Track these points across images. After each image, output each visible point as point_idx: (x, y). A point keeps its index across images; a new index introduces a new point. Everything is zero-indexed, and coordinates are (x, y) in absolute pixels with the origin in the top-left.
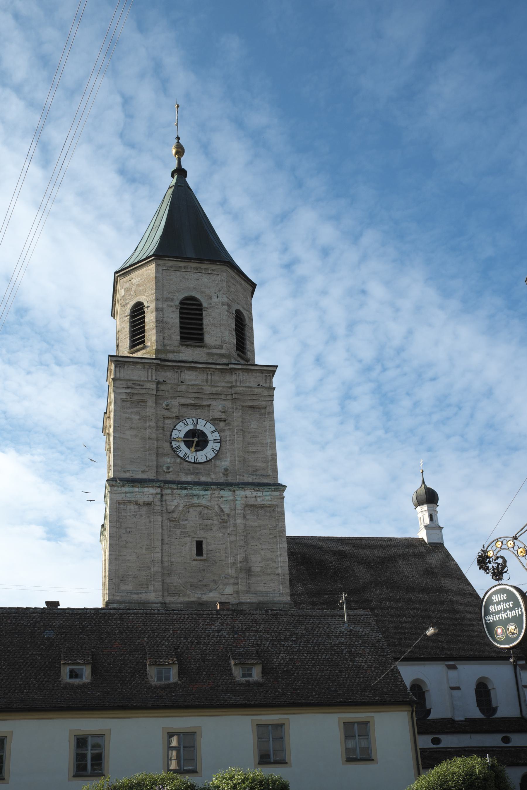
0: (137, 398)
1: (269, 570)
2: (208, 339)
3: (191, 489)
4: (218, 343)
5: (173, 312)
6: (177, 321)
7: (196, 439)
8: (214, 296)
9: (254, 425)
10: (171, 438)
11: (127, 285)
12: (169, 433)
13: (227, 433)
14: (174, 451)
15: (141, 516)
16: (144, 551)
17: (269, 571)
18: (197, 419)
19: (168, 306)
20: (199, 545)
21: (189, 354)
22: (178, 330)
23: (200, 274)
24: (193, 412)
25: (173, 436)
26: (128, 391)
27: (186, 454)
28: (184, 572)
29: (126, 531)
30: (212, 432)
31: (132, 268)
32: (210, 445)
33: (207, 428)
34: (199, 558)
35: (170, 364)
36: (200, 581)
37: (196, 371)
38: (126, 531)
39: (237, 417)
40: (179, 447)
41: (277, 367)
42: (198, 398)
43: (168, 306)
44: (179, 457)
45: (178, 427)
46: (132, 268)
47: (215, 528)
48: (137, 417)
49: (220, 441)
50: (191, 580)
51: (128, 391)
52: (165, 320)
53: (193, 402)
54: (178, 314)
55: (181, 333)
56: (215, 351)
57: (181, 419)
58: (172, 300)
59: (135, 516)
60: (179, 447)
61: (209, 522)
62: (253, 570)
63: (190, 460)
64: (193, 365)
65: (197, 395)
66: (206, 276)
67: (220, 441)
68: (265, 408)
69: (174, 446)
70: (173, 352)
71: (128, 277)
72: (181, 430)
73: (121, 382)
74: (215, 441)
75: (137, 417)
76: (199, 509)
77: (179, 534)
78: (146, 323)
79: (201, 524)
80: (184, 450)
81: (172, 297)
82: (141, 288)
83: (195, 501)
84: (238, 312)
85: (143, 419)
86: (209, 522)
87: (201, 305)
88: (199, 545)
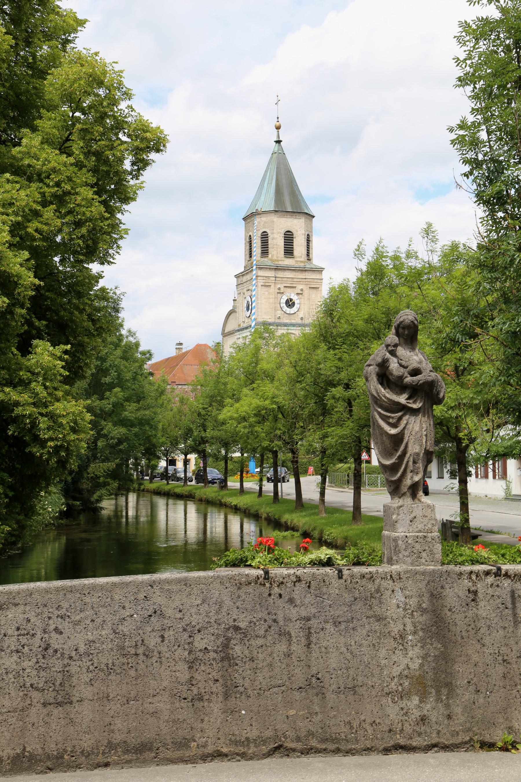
0: (267, 284)
2: (296, 253)
9: (313, 296)
21: (288, 262)
24: (289, 290)
32: (296, 306)
33: (295, 298)
39: (306, 292)
49: (300, 304)
56: (298, 259)
67: (300, 304)
72: (284, 299)
80: (285, 308)
83: (290, 331)
84: (308, 235)
85: (269, 293)
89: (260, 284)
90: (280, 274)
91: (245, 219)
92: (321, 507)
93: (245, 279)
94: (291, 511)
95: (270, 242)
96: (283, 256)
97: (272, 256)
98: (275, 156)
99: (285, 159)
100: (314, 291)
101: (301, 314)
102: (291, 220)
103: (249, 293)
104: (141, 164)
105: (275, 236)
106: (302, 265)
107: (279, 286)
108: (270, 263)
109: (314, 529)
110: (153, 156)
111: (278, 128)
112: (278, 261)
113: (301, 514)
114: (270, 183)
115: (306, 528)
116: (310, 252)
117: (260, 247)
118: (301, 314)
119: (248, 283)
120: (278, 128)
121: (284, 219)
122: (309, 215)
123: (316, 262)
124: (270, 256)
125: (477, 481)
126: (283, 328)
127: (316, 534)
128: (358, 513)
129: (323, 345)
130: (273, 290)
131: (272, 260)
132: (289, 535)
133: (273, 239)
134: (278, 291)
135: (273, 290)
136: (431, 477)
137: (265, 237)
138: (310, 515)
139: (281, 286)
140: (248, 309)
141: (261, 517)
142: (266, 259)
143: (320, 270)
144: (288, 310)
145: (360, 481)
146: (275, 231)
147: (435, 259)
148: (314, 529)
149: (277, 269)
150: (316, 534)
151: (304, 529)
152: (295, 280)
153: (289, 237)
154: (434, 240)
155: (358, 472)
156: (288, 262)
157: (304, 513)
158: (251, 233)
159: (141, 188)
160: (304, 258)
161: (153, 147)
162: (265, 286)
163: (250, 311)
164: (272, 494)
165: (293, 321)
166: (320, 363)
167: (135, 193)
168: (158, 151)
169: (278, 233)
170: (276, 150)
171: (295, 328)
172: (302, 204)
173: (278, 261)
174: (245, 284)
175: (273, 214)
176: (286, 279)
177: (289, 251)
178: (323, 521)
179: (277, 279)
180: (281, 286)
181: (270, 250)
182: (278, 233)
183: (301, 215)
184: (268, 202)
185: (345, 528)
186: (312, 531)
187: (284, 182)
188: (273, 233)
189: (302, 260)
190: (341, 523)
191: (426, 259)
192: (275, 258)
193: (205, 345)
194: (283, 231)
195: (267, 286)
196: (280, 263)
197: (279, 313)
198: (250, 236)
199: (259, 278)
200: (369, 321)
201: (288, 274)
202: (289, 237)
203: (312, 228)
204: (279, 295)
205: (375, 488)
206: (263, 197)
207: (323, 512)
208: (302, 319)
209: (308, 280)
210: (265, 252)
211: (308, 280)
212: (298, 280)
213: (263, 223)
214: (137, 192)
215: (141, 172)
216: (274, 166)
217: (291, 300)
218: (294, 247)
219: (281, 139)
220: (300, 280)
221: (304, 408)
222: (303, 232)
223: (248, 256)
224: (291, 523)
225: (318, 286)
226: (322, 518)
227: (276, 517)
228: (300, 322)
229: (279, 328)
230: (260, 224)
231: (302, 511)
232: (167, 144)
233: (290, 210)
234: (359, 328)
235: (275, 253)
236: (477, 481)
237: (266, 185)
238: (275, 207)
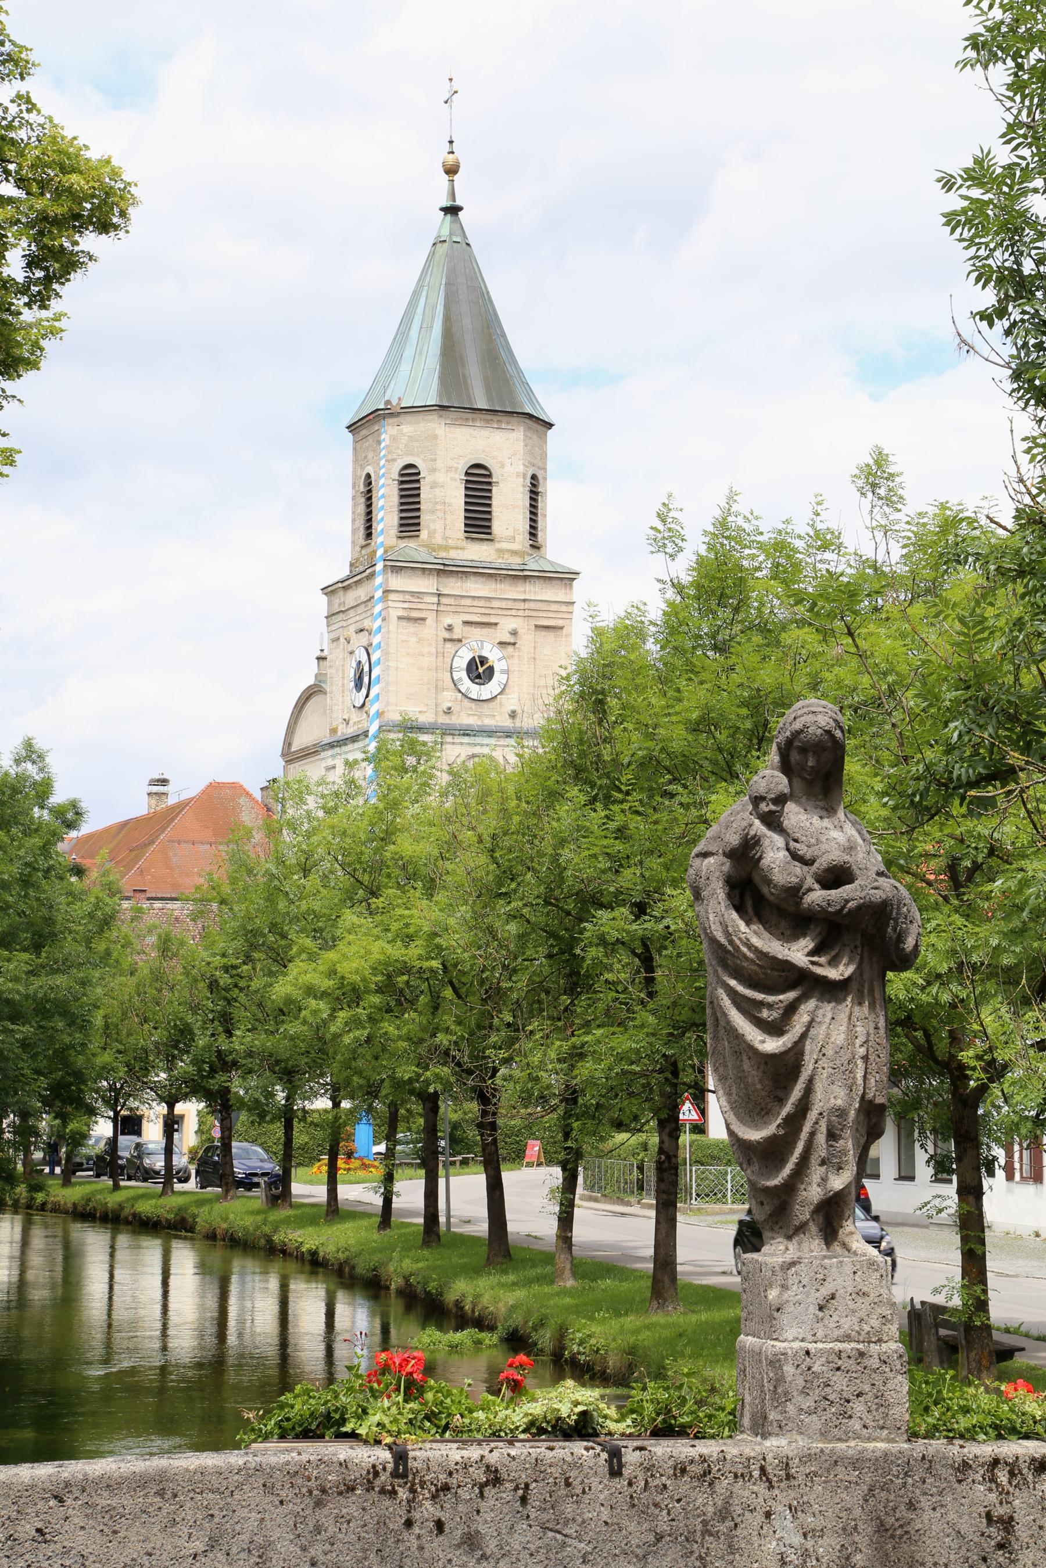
0: (415, 614)
2: (498, 527)
4: (509, 533)
6: (462, 500)
7: (481, 670)
13: (516, 661)
22: (462, 514)
24: (477, 632)
26: (406, 605)
32: (498, 677)
33: (493, 655)
39: (527, 638)
40: (460, 679)
43: (452, 479)
48: (414, 639)
49: (507, 672)
51: (406, 605)
54: (463, 492)
55: (466, 518)
56: (505, 546)
57: (464, 641)
58: (456, 469)
60: (460, 679)
65: (483, 611)
66: (498, 432)
67: (507, 672)
68: (562, 628)
70: (457, 548)
72: (465, 656)
74: (502, 672)
75: (414, 639)
80: (466, 684)
82: (415, 444)
84: (534, 477)
85: (420, 641)
87: (490, 476)
89: (394, 614)
90: (453, 586)
91: (352, 428)
92: (562, 1261)
93: (351, 597)
94: (475, 1271)
95: (426, 494)
96: (462, 535)
97: (431, 535)
98: (442, 249)
99: (472, 258)
100: (550, 636)
101: (510, 702)
102: (485, 432)
103: (363, 639)
104: (55, 265)
105: (441, 477)
106: (515, 561)
107: (448, 620)
108: (423, 555)
109: (541, 1324)
110: (89, 241)
111: (451, 170)
112: (447, 548)
113: (504, 1279)
114: (426, 328)
115: (517, 1320)
116: (540, 525)
117: (396, 509)
118: (510, 702)
119: (362, 608)
120: (451, 170)
121: (465, 429)
122: (538, 420)
123: (557, 551)
124: (424, 534)
125: (1009, 1191)
126: (458, 739)
127: (545, 1339)
128: (666, 1279)
129: (573, 791)
130: (432, 630)
131: (430, 548)
132: (469, 1342)
133: (434, 485)
134: (447, 635)
135: (432, 630)
136: (877, 1176)
137: (410, 481)
138: (529, 1282)
139: (456, 621)
140: (358, 686)
141: (388, 1288)
142: (412, 544)
143: (566, 578)
144: (475, 690)
145: (675, 1183)
146: (439, 464)
147: (893, 555)
148: (541, 1324)
149: (445, 571)
150: (545, 1339)
151: (512, 1323)
152: (496, 604)
153: (479, 484)
154: (893, 500)
155: (668, 1158)
157: (511, 1278)
158: (370, 469)
159: (54, 332)
160: (522, 541)
161: (90, 217)
162: (409, 619)
163: (364, 691)
164: (421, 1220)
165: (489, 722)
166: (562, 842)
167: (36, 346)
168: (105, 227)
169: (449, 469)
170: (445, 233)
172: (519, 388)
173: (447, 548)
174: (352, 613)
175: (434, 416)
176: (468, 602)
177: (478, 522)
178: (568, 1300)
179: (444, 600)
180: (456, 621)
181: (425, 518)
182: (449, 469)
183: (515, 419)
184: (419, 381)
185: (630, 1321)
186: (535, 1328)
187: (467, 324)
188: (434, 470)
189: (516, 546)
190: (619, 1307)
191: (868, 552)
192: (438, 540)
193: (237, 789)
194: (463, 465)
195: (416, 620)
196: (453, 554)
197: (449, 698)
198: (368, 476)
200: (704, 724)
202: (479, 484)
203: (544, 457)
204: (448, 645)
205: (718, 1207)
206: (405, 368)
207: (567, 1273)
208: (513, 715)
209: (532, 605)
210: (410, 521)
211: (532, 605)
212: (504, 605)
213: (404, 440)
214: (43, 343)
215: (55, 286)
216: (438, 279)
217: (483, 660)
218: (496, 509)
219: (459, 202)
220: (510, 605)
221: (515, 971)
222: (521, 469)
223: (362, 533)
224: (474, 1305)
225: (560, 623)
226: (564, 1292)
227: (432, 1287)
228: (507, 723)
229: (449, 739)
230: (398, 445)
231: (505, 1272)
232: (131, 211)
233: (482, 404)
234: (675, 746)
235: (438, 526)
236: (1009, 1191)
237: (414, 332)
238: (440, 395)
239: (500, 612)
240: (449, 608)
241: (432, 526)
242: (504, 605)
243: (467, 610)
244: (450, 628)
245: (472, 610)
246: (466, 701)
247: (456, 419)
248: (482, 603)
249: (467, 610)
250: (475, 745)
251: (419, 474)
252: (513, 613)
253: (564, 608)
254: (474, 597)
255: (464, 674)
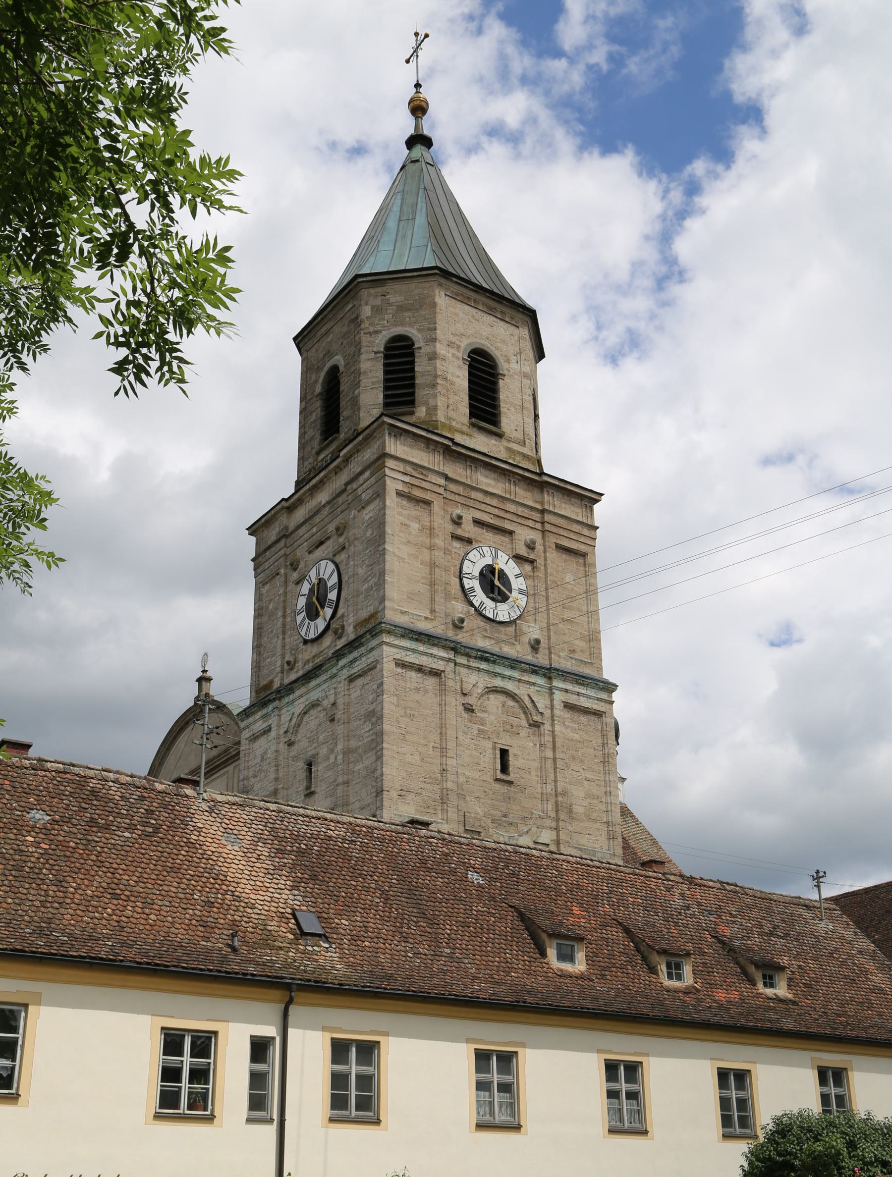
0: (417, 493)
1: (594, 814)
3: (494, 662)
5: (459, 367)
6: (466, 384)
8: (513, 359)
10: (461, 572)
11: (378, 301)
12: (458, 563)
14: (466, 595)
15: (426, 691)
16: (431, 752)
17: (594, 815)
18: (496, 549)
19: (454, 355)
20: (504, 753)
21: (480, 442)
23: (495, 319)
24: (489, 536)
25: (465, 570)
26: (407, 479)
27: (482, 603)
28: (482, 796)
29: (405, 713)
30: (517, 576)
31: (391, 276)
34: (504, 777)
35: (463, 451)
36: (505, 816)
37: (495, 472)
38: (405, 713)
40: (472, 589)
41: (602, 495)
42: (498, 516)
43: (454, 355)
44: (472, 605)
45: (470, 556)
46: (391, 276)
47: (523, 733)
48: (417, 526)
50: (492, 812)
51: (407, 479)
52: (449, 377)
53: (492, 522)
57: (475, 545)
59: (418, 690)
60: (472, 589)
61: (515, 721)
62: (574, 810)
63: (487, 614)
64: (493, 462)
65: (496, 512)
66: (502, 323)
69: (467, 587)
70: (463, 433)
71: (380, 289)
73: (395, 462)
74: (521, 592)
76: (502, 698)
77: (476, 732)
78: (417, 374)
79: (505, 723)
80: (479, 597)
81: (458, 343)
83: (498, 682)
86: (515, 721)
88: (504, 753)
101: (533, 631)
124: (421, 412)
126: (474, 664)
144: (490, 607)
152: (511, 507)
153: (483, 373)
156: (480, 442)
162: (409, 498)
169: (451, 344)
171: (516, 674)
194: (466, 344)
196: (459, 438)
197: (459, 608)
199: (390, 463)
201: (485, 480)
202: (483, 373)
204: (456, 544)
208: (535, 646)
212: (520, 511)
218: (504, 407)
225: (583, 548)
239: (515, 519)
240: (457, 498)
241: (432, 402)
242: (520, 511)
243: (477, 505)
244: (457, 521)
245: (483, 507)
246: (480, 619)
247: (457, 294)
248: (495, 502)
249: (477, 505)
250: (496, 675)
251: (413, 344)
252: (531, 523)
253: (586, 532)
254: (486, 493)
255: (476, 584)
